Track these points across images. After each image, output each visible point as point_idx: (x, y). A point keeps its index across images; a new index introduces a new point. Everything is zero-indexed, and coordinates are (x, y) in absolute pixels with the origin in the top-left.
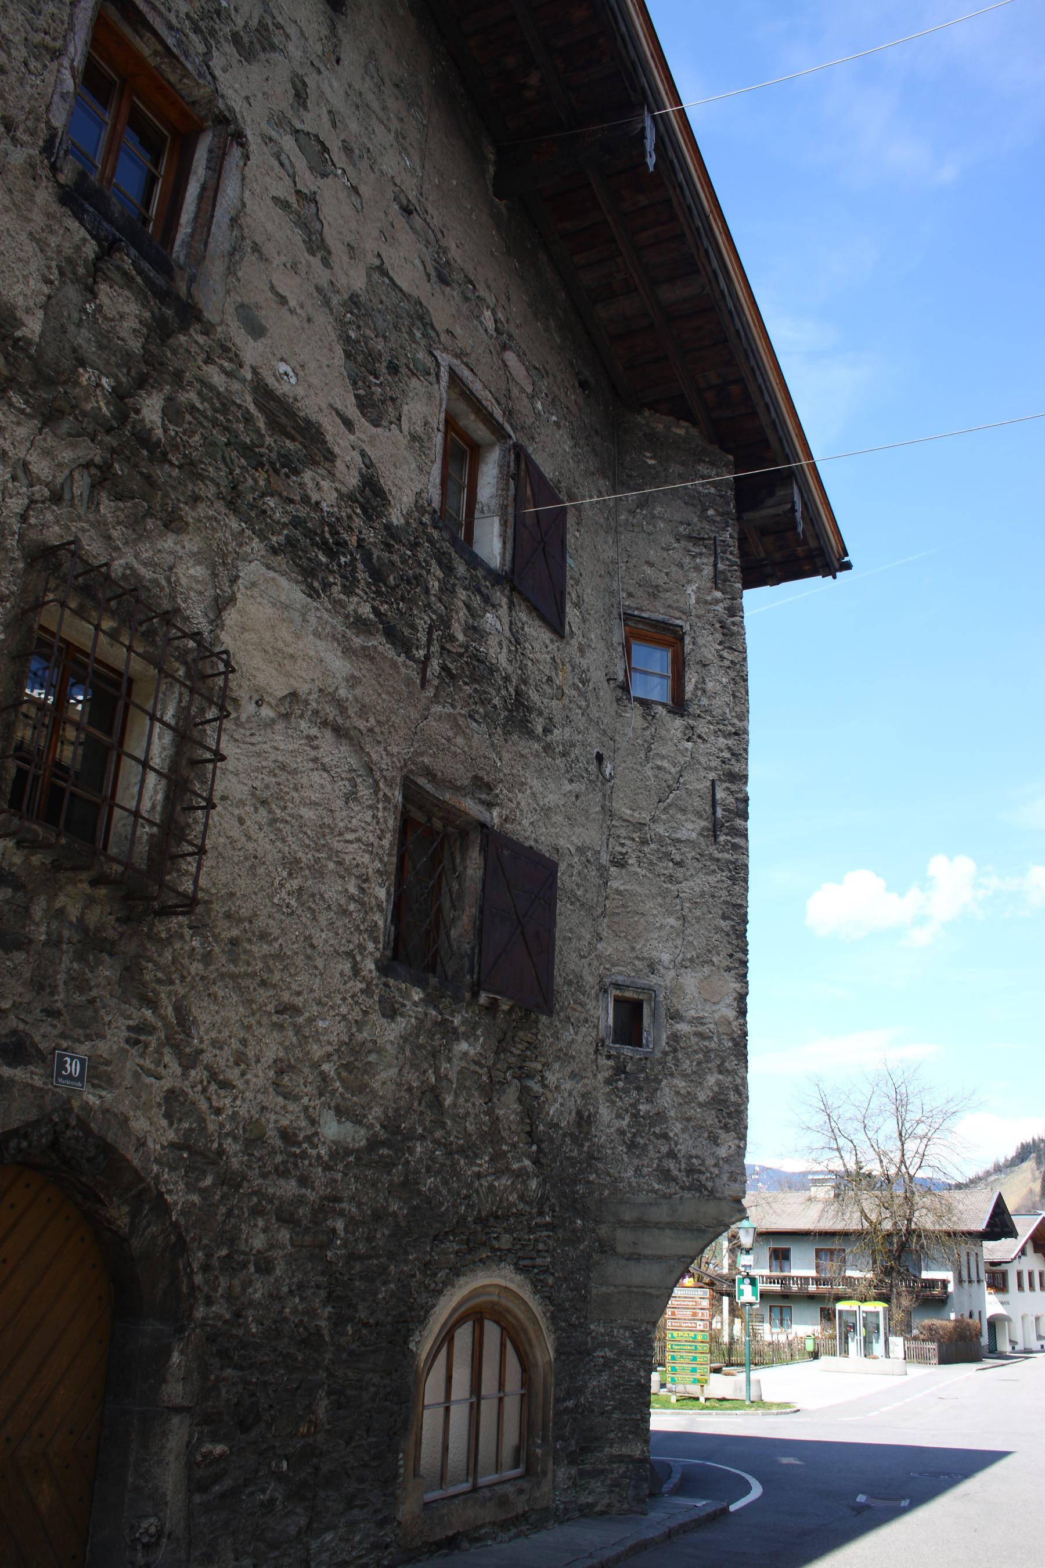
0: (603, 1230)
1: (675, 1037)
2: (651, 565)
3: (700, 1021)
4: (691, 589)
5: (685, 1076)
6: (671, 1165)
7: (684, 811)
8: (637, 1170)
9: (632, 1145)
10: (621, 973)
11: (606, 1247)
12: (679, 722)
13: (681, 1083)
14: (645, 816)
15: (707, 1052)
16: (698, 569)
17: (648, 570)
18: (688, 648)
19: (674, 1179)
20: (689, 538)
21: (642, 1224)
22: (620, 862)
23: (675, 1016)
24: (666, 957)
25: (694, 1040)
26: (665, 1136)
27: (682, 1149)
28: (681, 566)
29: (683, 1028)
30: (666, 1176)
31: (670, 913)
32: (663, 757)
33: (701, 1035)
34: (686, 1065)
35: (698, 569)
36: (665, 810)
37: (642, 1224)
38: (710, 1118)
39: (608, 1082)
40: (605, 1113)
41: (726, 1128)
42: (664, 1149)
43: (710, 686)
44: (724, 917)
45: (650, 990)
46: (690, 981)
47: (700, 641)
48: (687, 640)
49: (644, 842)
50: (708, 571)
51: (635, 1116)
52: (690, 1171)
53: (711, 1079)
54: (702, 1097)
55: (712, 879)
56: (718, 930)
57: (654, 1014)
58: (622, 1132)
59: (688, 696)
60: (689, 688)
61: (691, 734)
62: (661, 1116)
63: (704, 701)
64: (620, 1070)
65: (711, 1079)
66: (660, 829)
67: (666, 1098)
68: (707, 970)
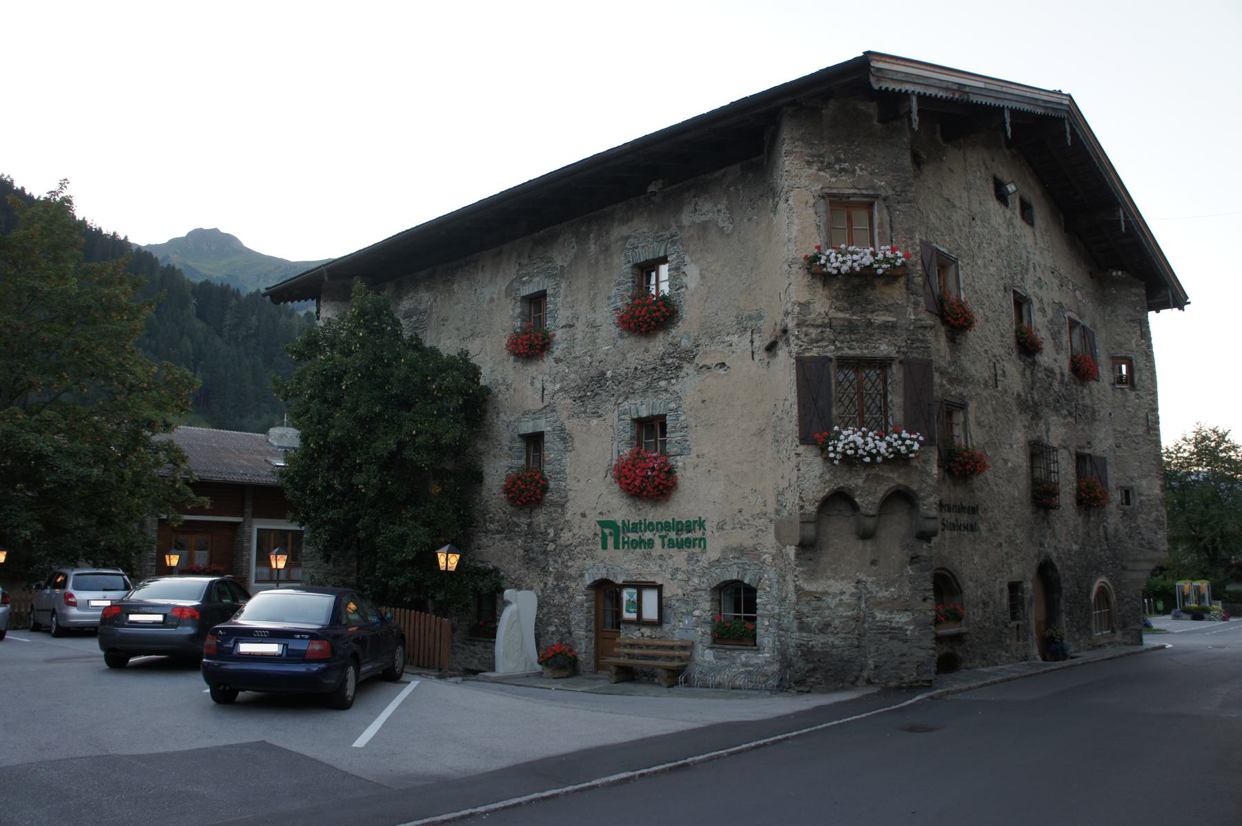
0: (1124, 563)
1: (1141, 502)
2: (1118, 335)
3: (1149, 495)
4: (1133, 342)
5: (1145, 513)
6: (1142, 542)
7: (1137, 425)
8: (1133, 544)
9: (1130, 537)
10: (1122, 483)
11: (1124, 568)
12: (1134, 393)
13: (1144, 516)
14: (1125, 429)
15: (1152, 505)
16: (1135, 333)
17: (1118, 337)
18: (1134, 364)
19: (1144, 546)
20: (1131, 321)
21: (1135, 561)
22: (1118, 446)
23: (1140, 495)
24: (1136, 475)
25: (1147, 502)
26: (1140, 533)
27: (1146, 537)
28: (1129, 333)
29: (1143, 498)
30: (1141, 545)
31: (1135, 461)
32: (1129, 407)
33: (1149, 500)
34: (1145, 510)
35: (1135, 333)
36: (1132, 426)
37: (1135, 561)
38: (1154, 526)
39: (1121, 518)
40: (1121, 527)
41: (1160, 529)
42: (1140, 537)
43: (1143, 377)
44: (1154, 460)
45: (1132, 488)
46: (1144, 482)
47: (1138, 361)
48: (1134, 361)
49: (1125, 438)
50: (1139, 332)
51: (1131, 528)
52: (1149, 543)
53: (1154, 514)
54: (1151, 520)
55: (1149, 447)
56: (1153, 464)
57: (1134, 495)
58: (1126, 533)
59: (1136, 383)
60: (1136, 379)
61: (1138, 396)
62: (1138, 527)
63: (1141, 384)
64: (1124, 514)
65: (1154, 514)
66: (1130, 433)
67: (1140, 521)
68: (1149, 478)
